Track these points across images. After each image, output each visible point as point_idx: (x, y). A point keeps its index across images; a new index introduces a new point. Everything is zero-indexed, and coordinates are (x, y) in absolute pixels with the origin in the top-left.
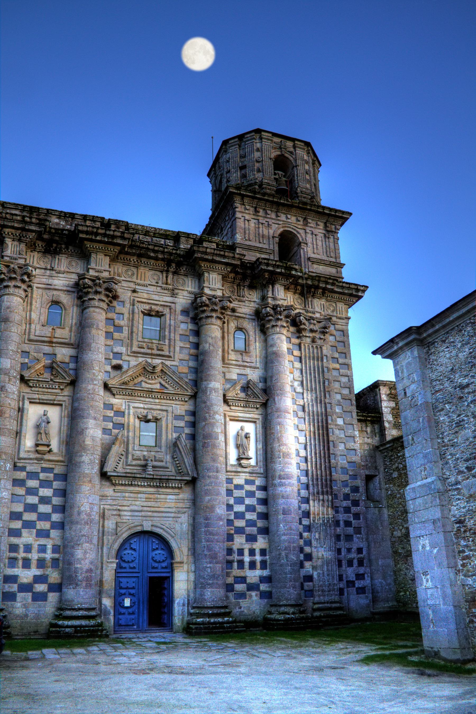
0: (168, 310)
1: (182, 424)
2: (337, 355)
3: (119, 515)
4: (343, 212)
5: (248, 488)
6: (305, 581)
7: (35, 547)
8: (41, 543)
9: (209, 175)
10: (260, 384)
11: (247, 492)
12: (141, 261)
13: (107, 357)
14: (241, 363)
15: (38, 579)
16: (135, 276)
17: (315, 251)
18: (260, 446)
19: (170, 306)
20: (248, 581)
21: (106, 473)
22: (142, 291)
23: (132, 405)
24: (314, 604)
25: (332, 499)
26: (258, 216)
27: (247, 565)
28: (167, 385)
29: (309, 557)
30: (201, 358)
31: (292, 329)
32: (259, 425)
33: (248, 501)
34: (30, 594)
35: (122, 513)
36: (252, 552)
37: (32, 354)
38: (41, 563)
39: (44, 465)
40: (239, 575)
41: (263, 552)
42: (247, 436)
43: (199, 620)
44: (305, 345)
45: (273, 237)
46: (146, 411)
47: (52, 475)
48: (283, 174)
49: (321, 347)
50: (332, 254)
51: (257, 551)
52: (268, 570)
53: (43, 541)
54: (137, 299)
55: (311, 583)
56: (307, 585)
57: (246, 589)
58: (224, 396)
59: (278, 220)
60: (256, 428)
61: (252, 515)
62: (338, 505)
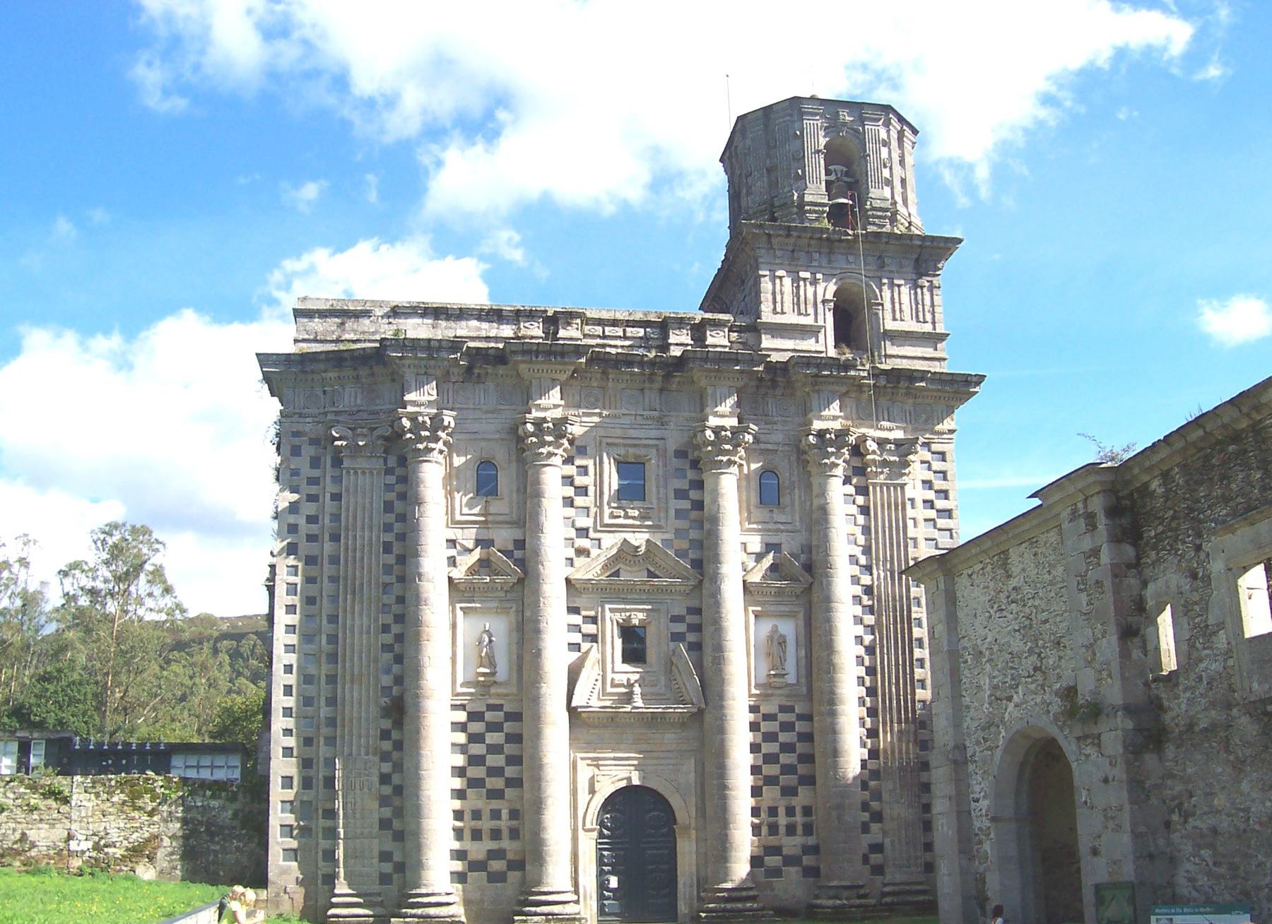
0: (655, 451)
1: (680, 628)
2: (930, 495)
3: (598, 766)
4: (947, 240)
5: (781, 717)
6: (871, 852)
7: (486, 814)
8: (495, 807)
9: (721, 160)
10: (802, 555)
11: (781, 723)
12: (608, 379)
13: (568, 536)
14: (771, 526)
15: (494, 854)
16: (600, 404)
17: (898, 316)
18: (802, 653)
19: (657, 445)
20: (785, 851)
21: (576, 708)
22: (613, 426)
23: (607, 607)
24: (885, 885)
25: (915, 731)
26: (797, 265)
27: (782, 830)
28: (657, 572)
29: (877, 817)
30: (707, 526)
31: (857, 462)
32: (801, 623)
33: (783, 737)
34: (485, 873)
35: (600, 762)
36: (790, 811)
37: (461, 541)
38: (496, 834)
39: (491, 701)
40: (770, 844)
41: (807, 811)
42: (782, 642)
43: (711, 905)
44: (874, 488)
45: (824, 302)
46: (628, 614)
47: (502, 713)
48: (845, 169)
49: (903, 486)
50: (929, 317)
51: (798, 810)
52: (814, 836)
53: (495, 804)
54: (605, 441)
55: (879, 855)
56: (875, 858)
57: (781, 863)
58: (744, 582)
59: (832, 268)
60: (797, 626)
61: (789, 757)
62: (927, 738)
